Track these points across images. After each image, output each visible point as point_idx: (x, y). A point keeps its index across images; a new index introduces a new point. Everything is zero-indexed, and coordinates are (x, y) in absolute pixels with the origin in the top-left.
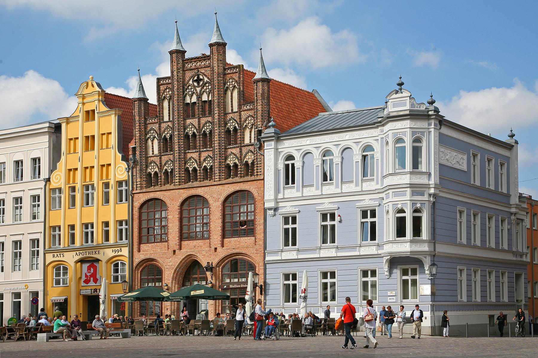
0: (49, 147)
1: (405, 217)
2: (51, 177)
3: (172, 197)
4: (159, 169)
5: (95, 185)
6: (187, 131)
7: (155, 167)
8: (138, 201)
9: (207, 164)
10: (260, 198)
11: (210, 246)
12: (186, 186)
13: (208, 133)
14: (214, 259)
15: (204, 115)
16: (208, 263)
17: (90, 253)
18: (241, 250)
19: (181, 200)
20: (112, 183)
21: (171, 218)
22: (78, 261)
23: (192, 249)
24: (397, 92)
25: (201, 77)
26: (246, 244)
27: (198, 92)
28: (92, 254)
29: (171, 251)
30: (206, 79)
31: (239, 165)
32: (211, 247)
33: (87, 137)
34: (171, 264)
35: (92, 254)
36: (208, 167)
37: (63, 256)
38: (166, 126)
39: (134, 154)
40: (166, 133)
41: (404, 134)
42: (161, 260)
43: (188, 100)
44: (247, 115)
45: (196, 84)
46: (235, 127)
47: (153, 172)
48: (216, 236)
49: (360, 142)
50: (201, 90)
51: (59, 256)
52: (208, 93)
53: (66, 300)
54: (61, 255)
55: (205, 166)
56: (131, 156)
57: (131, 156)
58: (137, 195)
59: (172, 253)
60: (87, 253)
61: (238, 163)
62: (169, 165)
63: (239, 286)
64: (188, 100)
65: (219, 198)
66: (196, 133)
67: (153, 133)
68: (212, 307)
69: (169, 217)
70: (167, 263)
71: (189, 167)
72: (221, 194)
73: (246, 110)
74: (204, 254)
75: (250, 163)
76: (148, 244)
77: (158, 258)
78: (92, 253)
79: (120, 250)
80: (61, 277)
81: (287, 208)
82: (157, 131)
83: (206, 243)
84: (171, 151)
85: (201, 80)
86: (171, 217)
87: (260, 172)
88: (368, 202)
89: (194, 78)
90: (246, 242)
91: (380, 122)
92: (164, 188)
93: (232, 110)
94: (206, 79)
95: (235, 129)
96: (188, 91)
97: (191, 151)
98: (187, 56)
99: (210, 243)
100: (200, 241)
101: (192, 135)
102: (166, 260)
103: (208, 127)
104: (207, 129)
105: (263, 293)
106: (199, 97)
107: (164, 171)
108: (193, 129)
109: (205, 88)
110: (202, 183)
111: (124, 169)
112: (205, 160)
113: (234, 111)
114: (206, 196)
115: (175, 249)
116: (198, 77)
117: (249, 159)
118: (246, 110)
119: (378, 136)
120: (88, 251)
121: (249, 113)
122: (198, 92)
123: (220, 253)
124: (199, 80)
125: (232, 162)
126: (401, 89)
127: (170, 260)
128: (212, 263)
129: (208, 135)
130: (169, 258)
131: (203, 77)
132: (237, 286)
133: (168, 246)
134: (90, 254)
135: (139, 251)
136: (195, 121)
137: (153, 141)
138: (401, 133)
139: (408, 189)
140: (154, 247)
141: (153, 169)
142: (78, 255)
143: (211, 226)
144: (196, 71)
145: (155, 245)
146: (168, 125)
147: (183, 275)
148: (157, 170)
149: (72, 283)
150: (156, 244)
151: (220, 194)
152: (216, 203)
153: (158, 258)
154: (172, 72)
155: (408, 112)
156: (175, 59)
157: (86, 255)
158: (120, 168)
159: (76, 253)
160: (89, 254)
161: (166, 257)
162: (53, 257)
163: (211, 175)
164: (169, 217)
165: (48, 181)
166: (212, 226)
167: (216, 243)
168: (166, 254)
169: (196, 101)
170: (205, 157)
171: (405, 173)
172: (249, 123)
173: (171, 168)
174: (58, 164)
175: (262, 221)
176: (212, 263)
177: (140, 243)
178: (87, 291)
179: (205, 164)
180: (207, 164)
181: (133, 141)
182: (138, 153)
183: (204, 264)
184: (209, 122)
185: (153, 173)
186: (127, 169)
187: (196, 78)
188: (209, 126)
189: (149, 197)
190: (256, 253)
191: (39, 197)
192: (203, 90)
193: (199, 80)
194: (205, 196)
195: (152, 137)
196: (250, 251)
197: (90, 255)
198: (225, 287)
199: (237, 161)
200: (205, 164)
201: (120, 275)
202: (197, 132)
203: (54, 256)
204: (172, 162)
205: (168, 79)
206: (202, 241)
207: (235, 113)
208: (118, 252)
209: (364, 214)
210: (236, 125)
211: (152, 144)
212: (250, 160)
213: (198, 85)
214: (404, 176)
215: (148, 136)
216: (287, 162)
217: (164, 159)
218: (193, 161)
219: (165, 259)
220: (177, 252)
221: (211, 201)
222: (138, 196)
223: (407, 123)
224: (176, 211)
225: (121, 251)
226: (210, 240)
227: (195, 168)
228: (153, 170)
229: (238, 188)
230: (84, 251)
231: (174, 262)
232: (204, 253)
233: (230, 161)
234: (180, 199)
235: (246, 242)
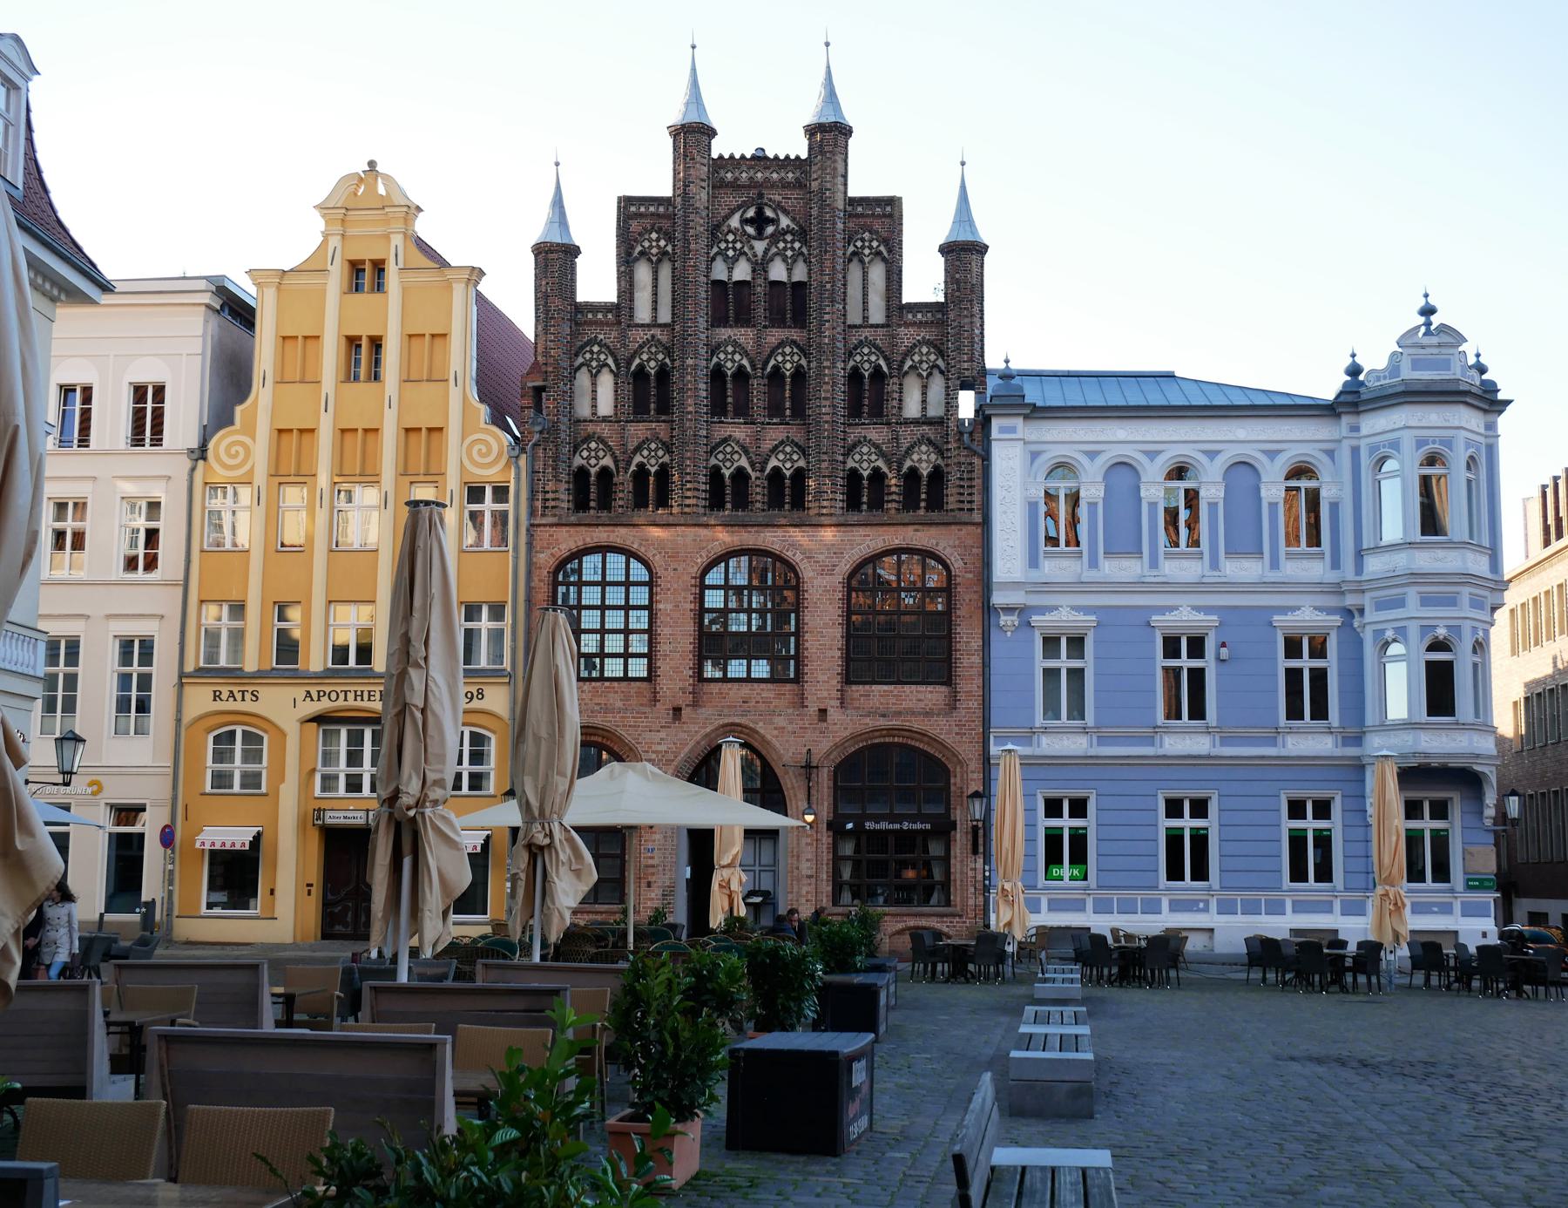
0: (203, 354)
3: (672, 549)
7: (601, 454)
8: (549, 548)
9: (784, 461)
10: (970, 576)
13: (788, 373)
17: (362, 696)
18: (908, 721)
22: (312, 716)
23: (736, 706)
25: (769, 213)
26: (922, 705)
28: (369, 700)
29: (663, 708)
30: (785, 222)
31: (890, 475)
32: (807, 707)
33: (353, 342)
34: (660, 748)
35: (369, 700)
37: (254, 699)
40: (645, 357)
42: (629, 735)
44: (918, 338)
46: (878, 369)
47: (597, 468)
50: (766, 251)
51: (239, 696)
53: (257, 840)
54: (248, 696)
55: (776, 470)
58: (546, 532)
60: (351, 696)
61: (885, 469)
63: (897, 826)
65: (834, 566)
68: (810, 884)
69: (661, 606)
70: (652, 743)
72: (842, 553)
73: (913, 324)
74: (783, 723)
75: (925, 473)
77: (618, 726)
78: (369, 696)
79: (479, 693)
81: (1064, 617)
83: (784, 694)
84: (660, 411)
86: (669, 607)
87: (968, 502)
89: (744, 212)
90: (920, 700)
93: (865, 318)
94: (785, 222)
95: (877, 373)
97: (730, 420)
98: (719, 148)
101: (733, 375)
102: (648, 735)
103: (788, 358)
104: (784, 362)
105: (981, 849)
106: (760, 266)
107: (633, 468)
108: (737, 357)
109: (781, 245)
112: (774, 450)
113: (872, 321)
114: (789, 554)
115: (680, 702)
116: (760, 212)
117: (920, 460)
118: (913, 324)
120: (353, 688)
121: (922, 334)
122: (760, 252)
123: (835, 724)
124: (760, 221)
125: (865, 465)
127: (663, 734)
130: (659, 731)
131: (777, 215)
132: (891, 827)
134: (362, 700)
136: (745, 336)
137: (594, 377)
140: (602, 692)
141: (596, 460)
142: (315, 698)
143: (807, 645)
144: (753, 193)
145: (606, 688)
148: (607, 461)
150: (607, 684)
151: (839, 554)
153: (618, 726)
157: (346, 700)
159: (308, 692)
160: (359, 698)
161: (646, 727)
162: (215, 700)
164: (661, 606)
166: (811, 644)
167: (825, 694)
168: (646, 717)
169: (749, 278)
172: (921, 362)
173: (661, 461)
174: (239, 409)
175: (976, 644)
178: (350, 814)
179: (773, 463)
180: (784, 461)
185: (593, 471)
187: (751, 213)
189: (588, 540)
190: (957, 734)
192: (774, 250)
193: (760, 221)
195: (594, 364)
196: (938, 725)
197: (359, 703)
198: (850, 826)
199: (880, 463)
200: (773, 463)
203: (217, 696)
205: (656, 204)
206: (770, 686)
207: (877, 326)
208: (471, 699)
210: (882, 362)
211: (594, 384)
212: (924, 465)
215: (580, 360)
216: (1052, 484)
217: (637, 431)
218: (736, 448)
221: (807, 571)
222: (551, 536)
224: (684, 590)
225: (480, 696)
227: (740, 470)
228: (593, 461)
229: (897, 542)
230: (338, 689)
231: (674, 744)
233: (861, 461)
235: (920, 700)
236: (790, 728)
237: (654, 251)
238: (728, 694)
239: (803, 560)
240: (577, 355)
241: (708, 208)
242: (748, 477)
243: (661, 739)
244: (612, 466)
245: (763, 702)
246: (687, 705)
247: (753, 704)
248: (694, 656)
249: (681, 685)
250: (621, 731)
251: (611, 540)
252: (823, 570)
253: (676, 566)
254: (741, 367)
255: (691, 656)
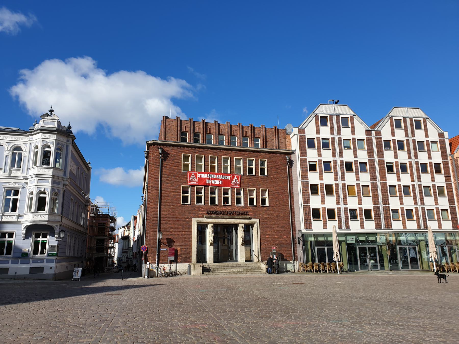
1: (46, 197)
24: (48, 115)
41: (52, 142)
49: (12, 143)
88: (12, 184)
91: (31, 132)
119: (28, 141)
126: (51, 114)
138: (49, 142)
139: (51, 179)
155: (55, 129)
171: (50, 168)
209: (8, 192)
214: (48, 170)
223: (54, 136)
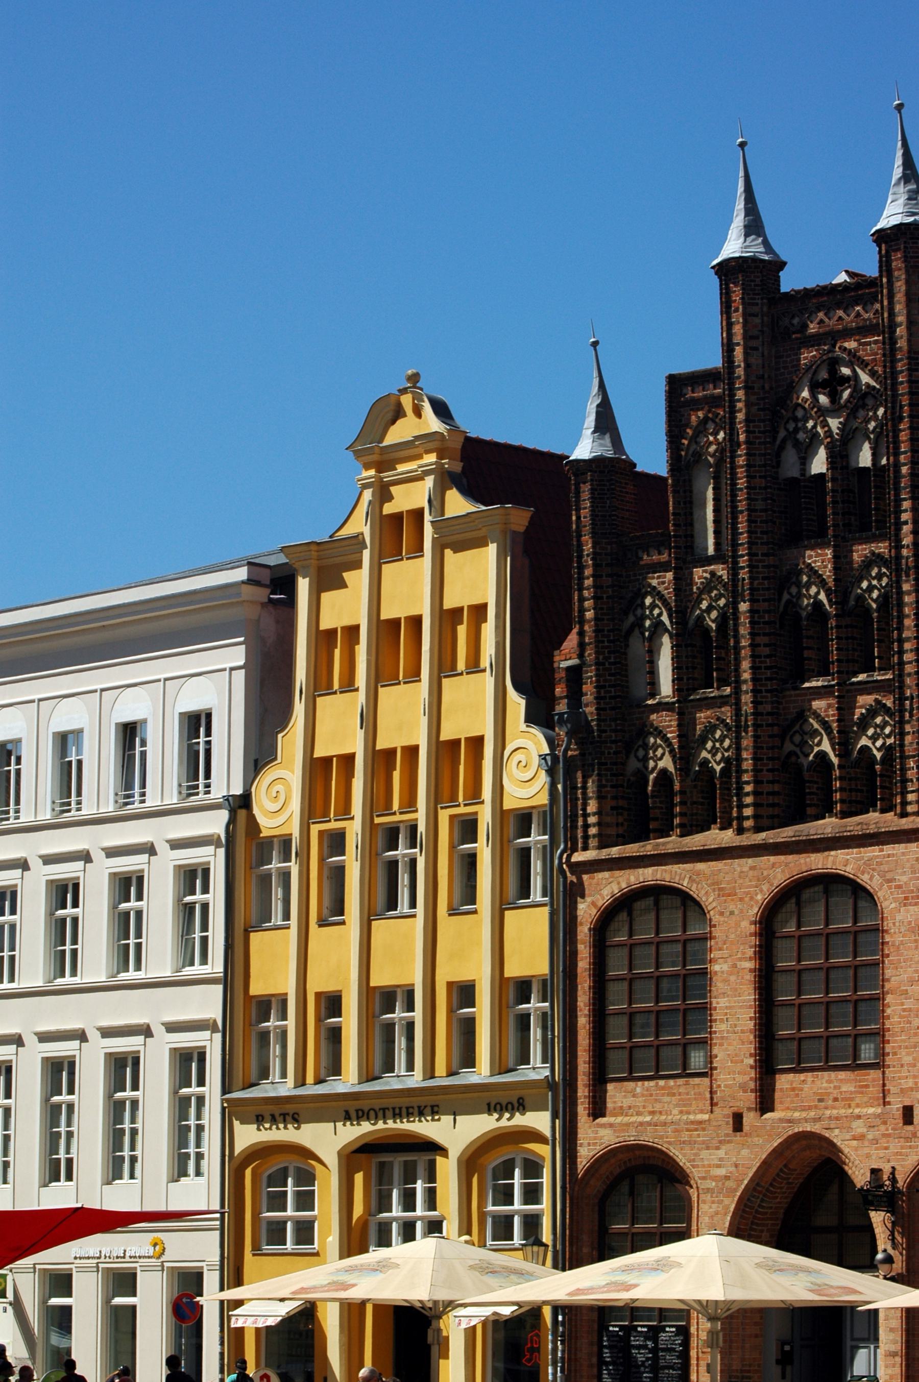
2: (253, 790)
4: (675, 763)
5: (422, 828)
6: (859, 591)
11: (884, 1097)
12: (786, 834)
13: (874, 606)
14: (901, 1154)
15: (866, 533)
16: (875, 1172)
19: (762, 896)
20: (485, 816)
21: (722, 972)
27: (835, 431)
29: (723, 1114)
32: (889, 1103)
34: (722, 1172)
36: (875, 752)
38: (706, 578)
39: (575, 696)
40: (704, 605)
43: (790, 469)
45: (823, 399)
48: (908, 1054)
52: (872, 436)
56: (562, 707)
57: (562, 707)
59: (727, 1123)
62: (718, 745)
64: (790, 469)
66: (828, 607)
67: (653, 606)
68: (894, 1366)
69: (716, 968)
70: (709, 1166)
71: (797, 750)
76: (631, 1085)
80: (290, 1212)
82: (667, 596)
83: (867, 1086)
85: (845, 380)
86: (725, 967)
92: (697, 841)
96: (791, 429)
98: (789, 282)
99: (884, 1085)
100: (842, 1075)
102: (704, 1154)
104: (871, 588)
109: (861, 413)
110: (854, 824)
111: (536, 761)
114: (866, 877)
127: (721, 1153)
128: (893, 1173)
129: (875, 614)
130: (718, 1148)
131: (854, 371)
133: (711, 1092)
135: (598, 1110)
143: (889, 1011)
145: (663, 1088)
146: (713, 574)
147: (779, 1222)
148: (666, 763)
149: (330, 1239)
150: (662, 1083)
152: (908, 911)
153: (669, 1143)
154: (728, 348)
156: (737, 297)
158: (518, 756)
161: (703, 1142)
163: (888, 788)
164: (716, 968)
165: (240, 807)
168: (704, 1129)
170: (864, 711)
173: (726, 754)
176: (893, 1173)
177: (599, 1080)
181: (572, 641)
182: (589, 690)
183: (860, 1177)
184: (880, 556)
186: (545, 759)
188: (879, 577)
191: (206, 872)
194: (864, 879)
201: (517, 1212)
202: (830, 601)
204: (729, 729)
213: (833, 401)
219: (698, 1149)
220: (749, 1119)
221: (887, 900)
226: (884, 1073)
232: (859, 1127)
234: (761, 891)
236: (870, 1137)
237: (712, 449)
238: (802, 1090)
239: (882, 885)
240: (626, 613)
241: (762, 377)
242: (830, 764)
243: (721, 1159)
244: (671, 768)
245: (843, 1099)
246: (749, 1109)
247: (830, 1102)
248: (755, 1037)
249: (740, 1079)
250: (675, 1152)
251: (659, 877)
252: (906, 898)
253: (732, 907)
254: (818, 604)
255: (752, 1037)
